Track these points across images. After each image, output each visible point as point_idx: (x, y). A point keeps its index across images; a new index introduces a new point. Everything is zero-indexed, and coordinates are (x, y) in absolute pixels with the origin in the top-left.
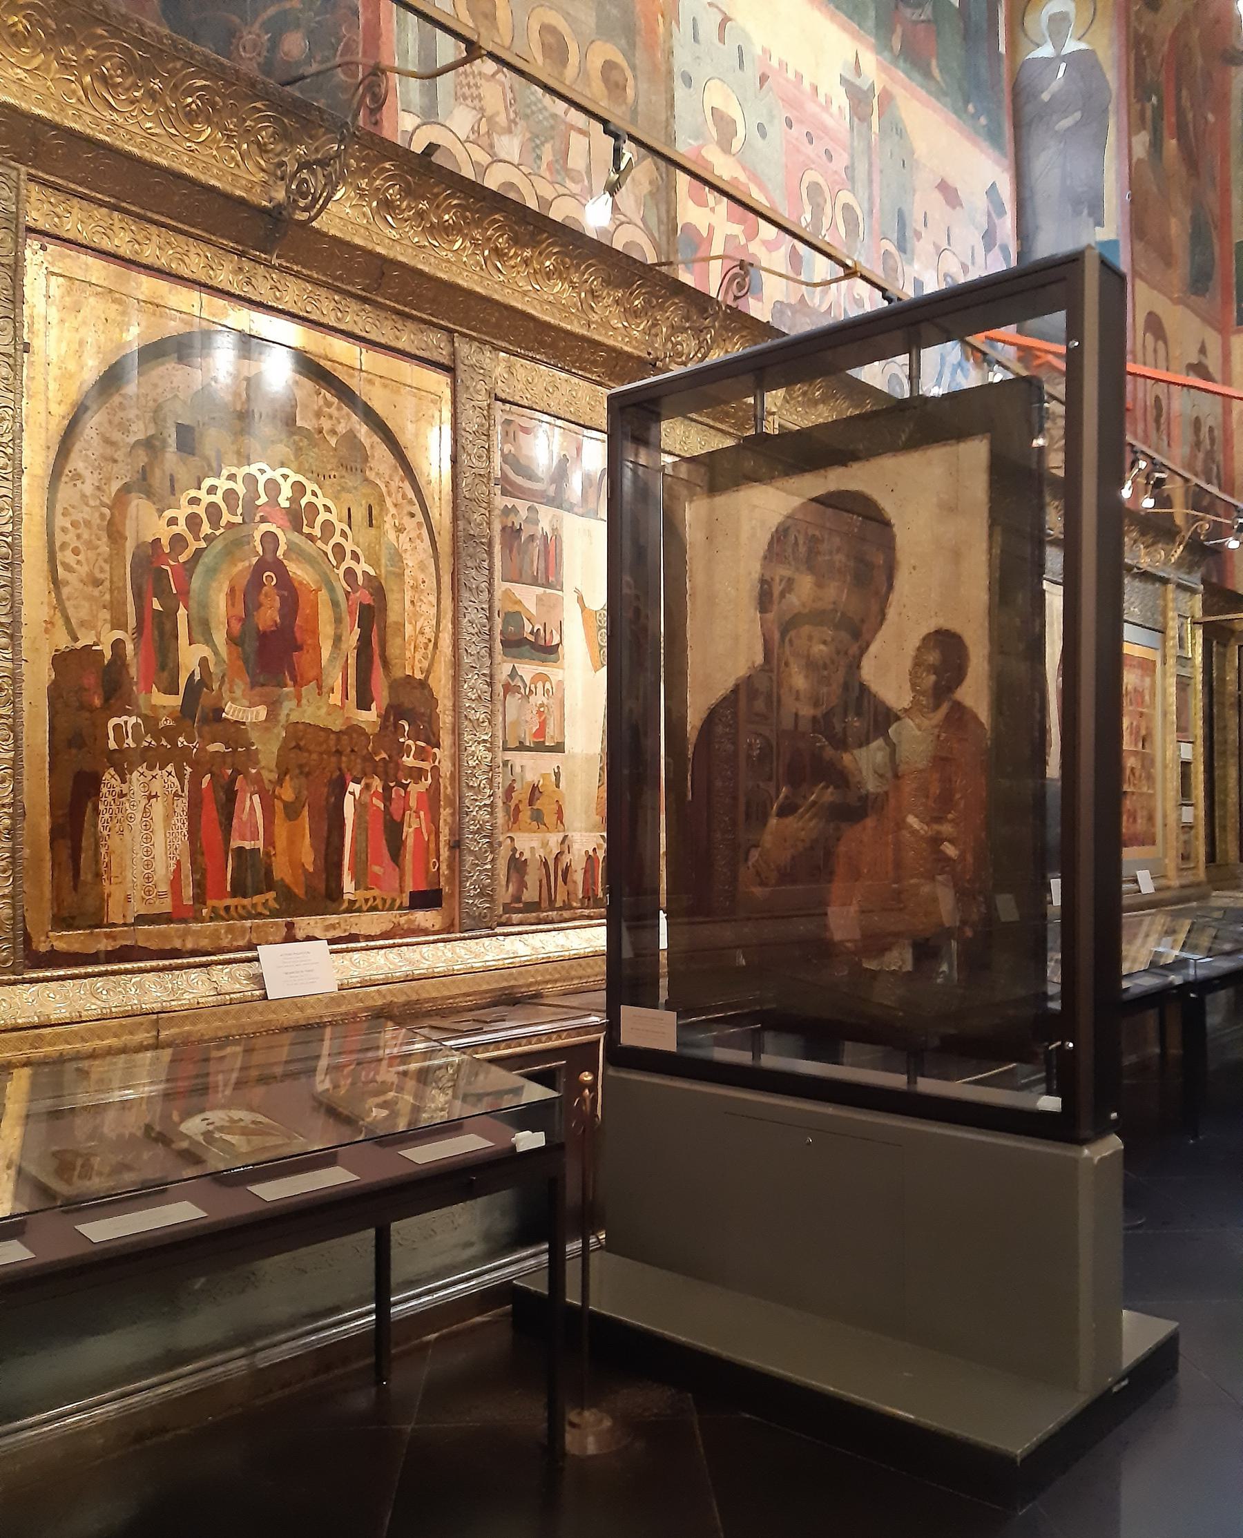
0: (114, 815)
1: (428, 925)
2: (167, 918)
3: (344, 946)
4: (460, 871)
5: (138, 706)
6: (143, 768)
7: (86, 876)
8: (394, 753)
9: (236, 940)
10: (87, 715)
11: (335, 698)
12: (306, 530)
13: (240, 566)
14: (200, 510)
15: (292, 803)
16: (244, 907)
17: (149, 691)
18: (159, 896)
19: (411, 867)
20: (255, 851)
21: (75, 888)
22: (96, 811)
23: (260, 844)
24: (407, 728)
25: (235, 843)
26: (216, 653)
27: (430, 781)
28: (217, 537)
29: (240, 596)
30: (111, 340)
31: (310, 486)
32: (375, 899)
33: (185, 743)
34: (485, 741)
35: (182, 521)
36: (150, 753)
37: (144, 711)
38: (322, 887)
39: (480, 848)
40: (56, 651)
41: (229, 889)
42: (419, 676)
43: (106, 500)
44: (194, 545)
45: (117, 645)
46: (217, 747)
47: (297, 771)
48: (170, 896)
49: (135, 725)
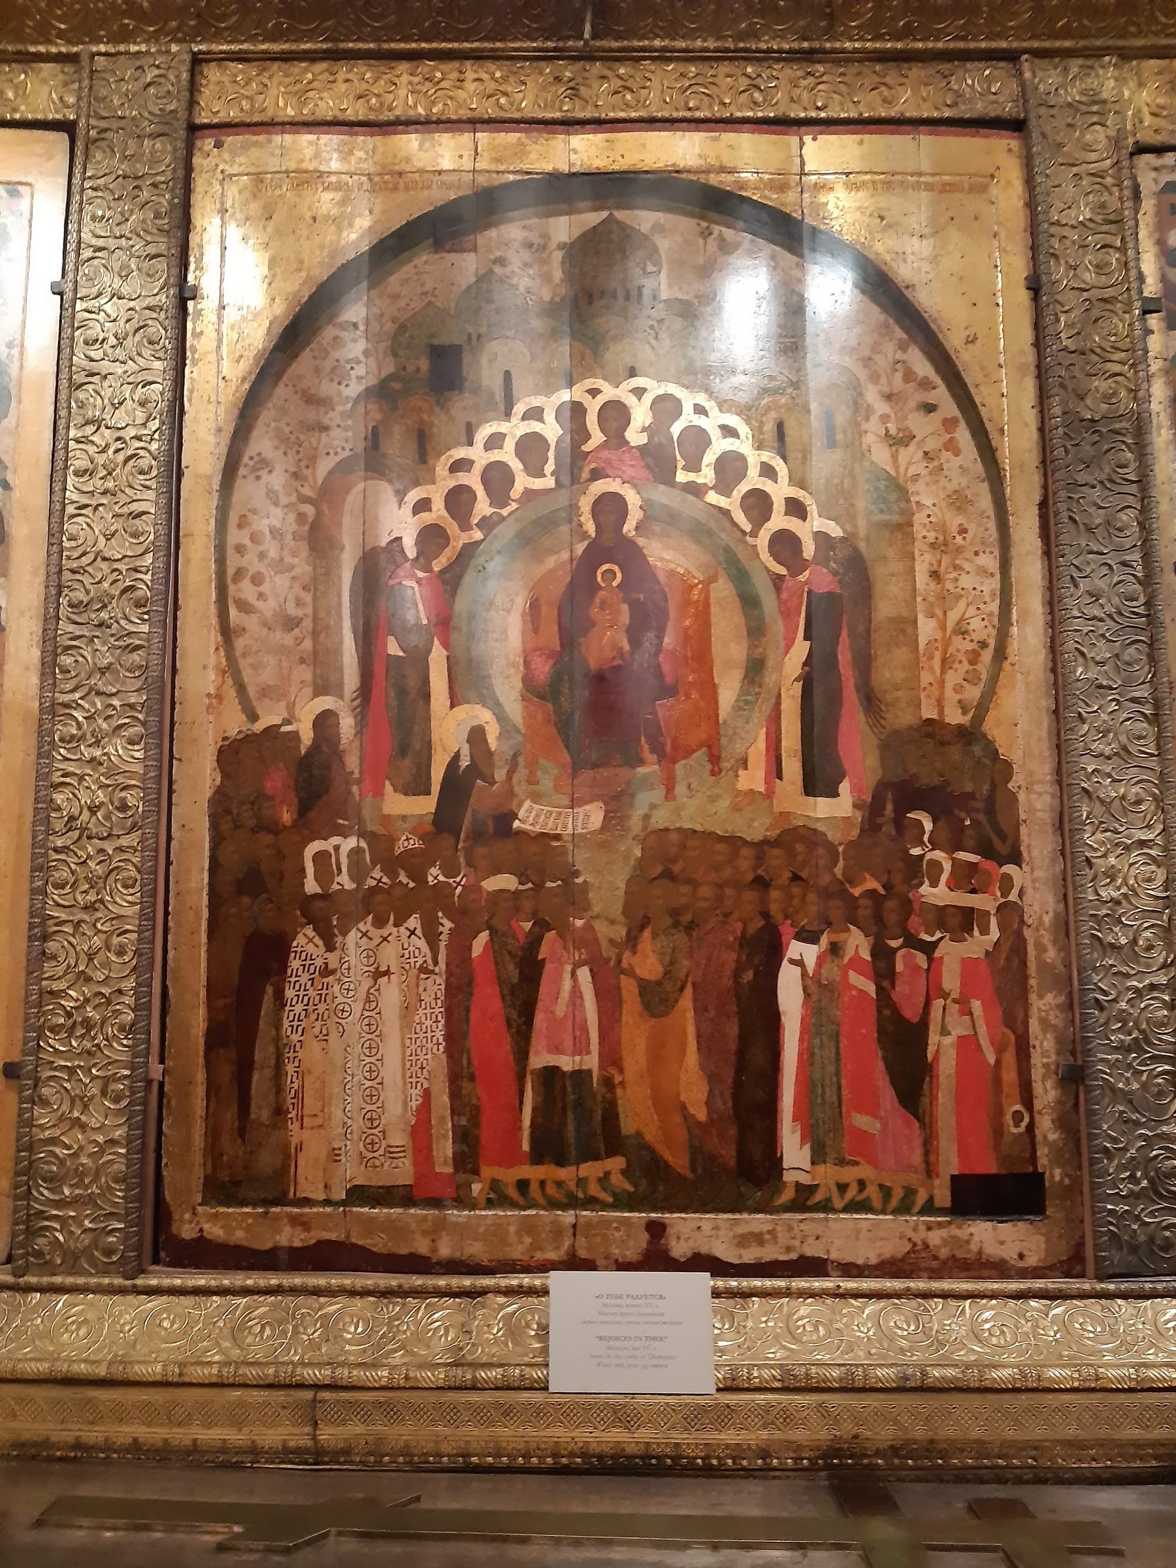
0: (311, 1008)
1: (1009, 1253)
2: (404, 1197)
3: (781, 1283)
4: (1091, 1137)
5: (360, 820)
6: (366, 925)
7: (260, 1111)
8: (897, 879)
9: (541, 1249)
10: (269, 839)
11: (753, 778)
12: (682, 477)
13: (551, 562)
14: (472, 480)
15: (659, 983)
16: (559, 1184)
17: (379, 793)
18: (390, 1152)
19: (953, 1121)
20: (581, 1076)
21: (242, 1132)
22: (280, 1001)
23: (592, 1062)
24: (928, 826)
25: (539, 1059)
26: (501, 717)
27: (995, 934)
28: (504, 519)
29: (549, 614)
30: (322, 247)
31: (688, 399)
32: (862, 1184)
33: (441, 878)
34: (1142, 843)
35: (438, 505)
36: (379, 898)
37: (370, 827)
38: (728, 1153)
39: (1145, 1086)
40: (225, 739)
41: (526, 1146)
42: (955, 717)
43: (307, 491)
44: (460, 539)
45: (325, 721)
46: (506, 882)
47: (668, 921)
48: (409, 1154)
49: (356, 852)
